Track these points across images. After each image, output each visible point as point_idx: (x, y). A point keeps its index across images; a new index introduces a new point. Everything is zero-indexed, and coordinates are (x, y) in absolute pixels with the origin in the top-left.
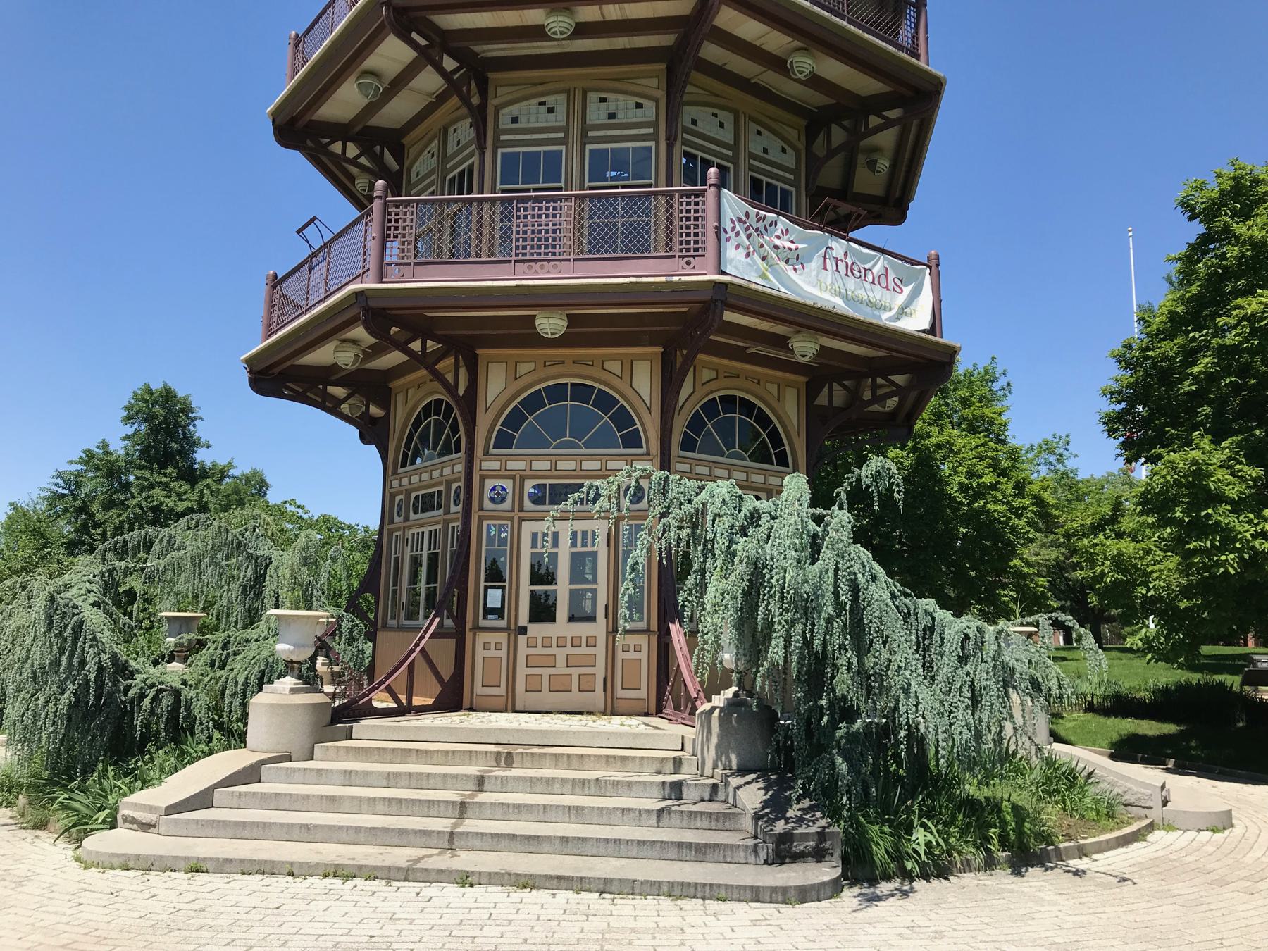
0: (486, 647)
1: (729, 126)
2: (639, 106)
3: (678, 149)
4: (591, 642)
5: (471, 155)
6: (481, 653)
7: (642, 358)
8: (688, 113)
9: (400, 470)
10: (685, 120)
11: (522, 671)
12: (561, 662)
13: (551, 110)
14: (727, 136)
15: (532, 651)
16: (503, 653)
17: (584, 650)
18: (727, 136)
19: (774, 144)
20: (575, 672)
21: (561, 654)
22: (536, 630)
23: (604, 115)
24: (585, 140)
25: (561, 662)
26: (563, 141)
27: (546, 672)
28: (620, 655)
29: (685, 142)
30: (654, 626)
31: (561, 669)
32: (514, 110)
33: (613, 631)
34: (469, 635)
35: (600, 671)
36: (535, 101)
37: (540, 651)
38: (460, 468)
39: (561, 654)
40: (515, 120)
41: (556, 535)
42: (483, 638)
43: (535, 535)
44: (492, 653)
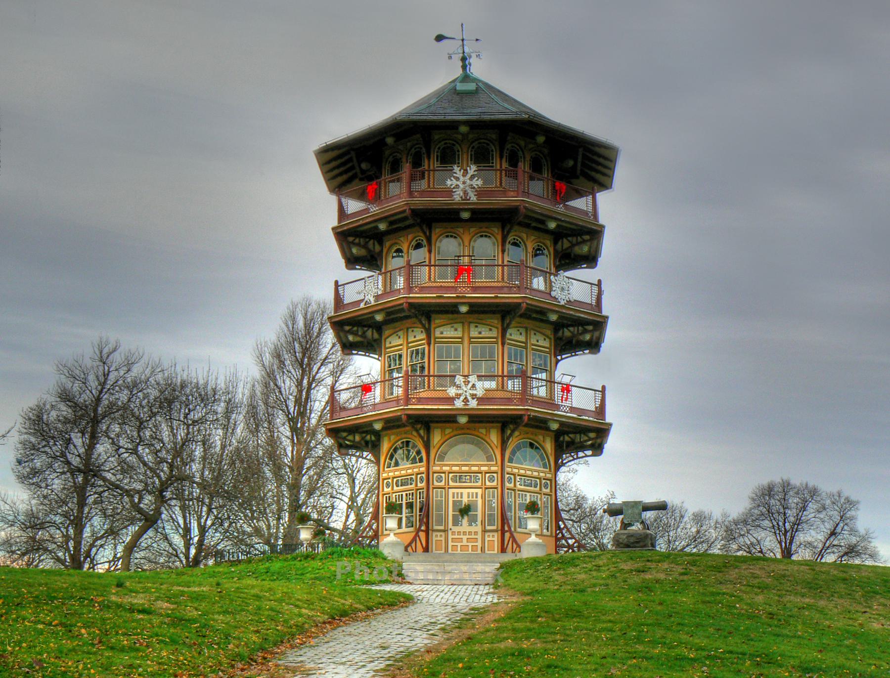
0: (437, 536)
1: (524, 334)
2: (491, 330)
3: (506, 346)
4: (476, 533)
5: (423, 344)
6: (434, 539)
7: (493, 427)
8: (509, 331)
9: (386, 469)
10: (508, 336)
11: (450, 544)
12: (465, 540)
13: (456, 330)
14: (523, 339)
15: (454, 537)
16: (443, 539)
17: (473, 536)
18: (523, 339)
19: (540, 337)
20: (470, 544)
21: (465, 538)
22: (456, 529)
23: (476, 333)
24: (470, 343)
25: (465, 540)
26: (461, 343)
27: (459, 544)
28: (487, 539)
29: (509, 344)
30: (500, 528)
31: (465, 543)
32: (441, 329)
33: (485, 531)
34: (430, 532)
35: (479, 544)
36: (449, 326)
37: (456, 536)
38: (423, 469)
39: (465, 538)
40: (442, 333)
41: (462, 494)
42: (435, 534)
43: (453, 494)
44: (439, 538)
